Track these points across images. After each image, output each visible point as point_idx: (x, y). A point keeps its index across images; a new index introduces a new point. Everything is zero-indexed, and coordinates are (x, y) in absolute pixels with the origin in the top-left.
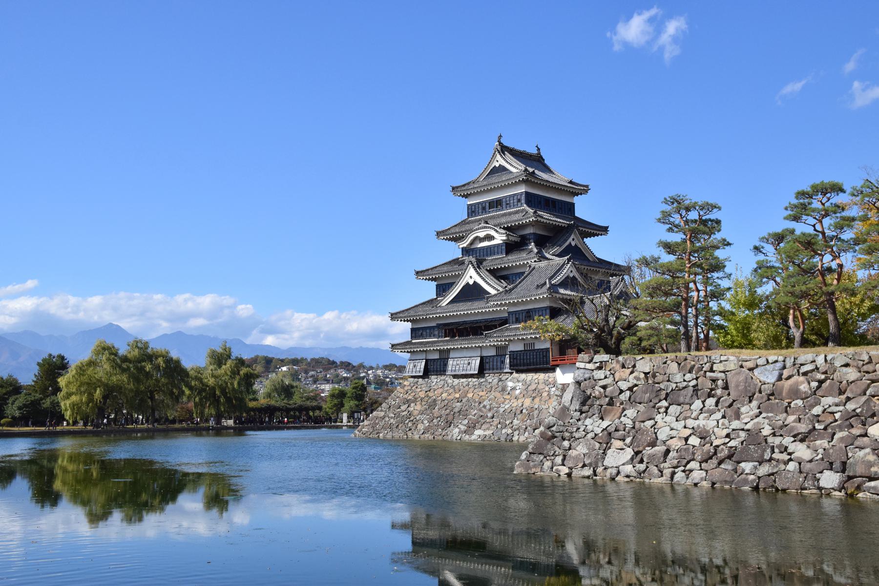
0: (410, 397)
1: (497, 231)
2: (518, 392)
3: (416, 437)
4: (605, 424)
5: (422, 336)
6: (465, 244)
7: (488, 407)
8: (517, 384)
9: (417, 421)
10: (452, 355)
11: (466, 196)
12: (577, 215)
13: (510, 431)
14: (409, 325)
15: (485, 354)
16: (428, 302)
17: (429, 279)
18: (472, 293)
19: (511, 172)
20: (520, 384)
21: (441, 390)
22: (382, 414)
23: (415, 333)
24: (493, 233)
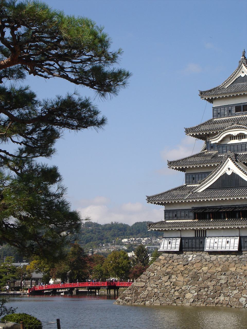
0: (170, 270)
3: (188, 304)
5: (176, 217)
9: (184, 291)
10: (208, 234)
11: (211, 101)
14: (163, 208)
16: (179, 188)
18: (230, 182)
21: (200, 264)
22: (143, 284)
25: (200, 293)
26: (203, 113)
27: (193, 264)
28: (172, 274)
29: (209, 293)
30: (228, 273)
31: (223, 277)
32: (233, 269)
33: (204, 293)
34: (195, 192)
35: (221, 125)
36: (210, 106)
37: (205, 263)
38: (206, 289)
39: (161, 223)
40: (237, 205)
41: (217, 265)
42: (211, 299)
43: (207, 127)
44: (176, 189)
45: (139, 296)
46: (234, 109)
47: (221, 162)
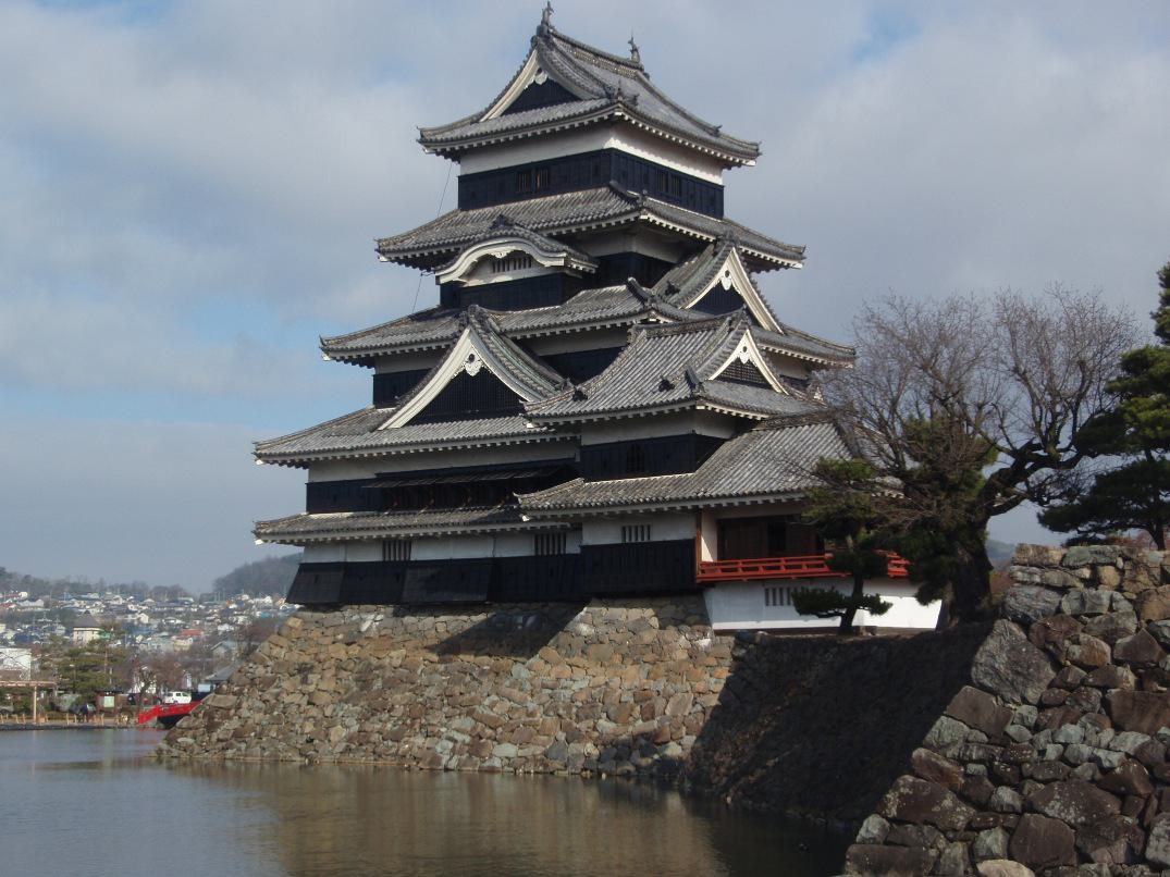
0: (306, 659)
4: (1133, 740)
11: (455, 155)
12: (727, 214)
14: (303, 476)
23: (319, 497)
24: (528, 250)
28: (311, 669)
29: (389, 725)
31: (437, 677)
33: (378, 726)
34: (385, 429)
36: (451, 171)
37: (400, 638)
38: (385, 716)
39: (295, 520)
40: (491, 465)
42: (390, 743)
44: (338, 421)
45: (215, 736)
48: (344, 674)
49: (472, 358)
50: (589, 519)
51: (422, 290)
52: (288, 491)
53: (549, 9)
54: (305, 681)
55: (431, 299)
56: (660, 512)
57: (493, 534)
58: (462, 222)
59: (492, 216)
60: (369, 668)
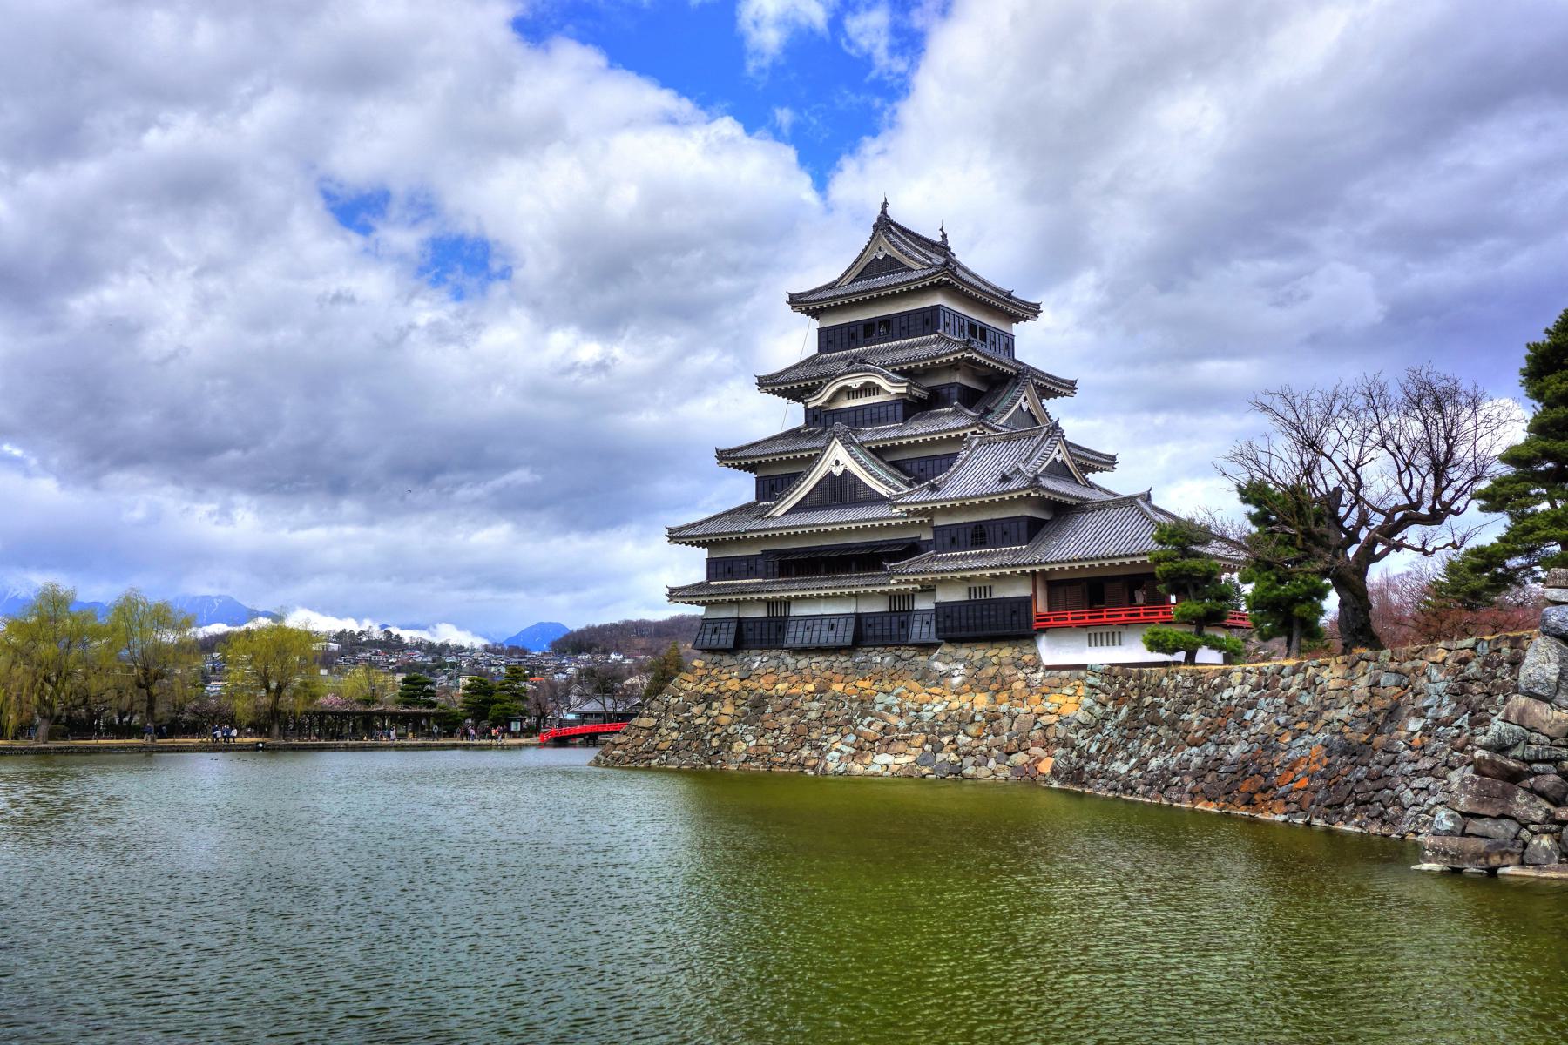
1: (888, 378)
2: (957, 680)
3: (733, 767)
6: (819, 400)
7: (896, 709)
8: (953, 666)
11: (815, 314)
13: (953, 757)
14: (704, 553)
15: (865, 608)
17: (740, 467)
18: (840, 491)
19: (910, 270)
20: (961, 666)
21: (773, 678)
22: (653, 722)
23: (715, 568)
25: (762, 741)
26: (796, 341)
27: (760, 677)
28: (716, 699)
30: (827, 696)
31: (815, 704)
32: (838, 687)
35: (831, 367)
39: (699, 586)
41: (808, 678)
43: (801, 373)
44: (729, 512)
46: (861, 328)
47: (824, 449)
48: (739, 702)
49: (837, 463)
50: (943, 581)
51: (790, 415)
52: (692, 566)
53: (885, 205)
54: (709, 707)
55: (800, 421)
56: (1003, 575)
57: (857, 595)
58: (822, 362)
59: (846, 357)
60: (762, 697)
